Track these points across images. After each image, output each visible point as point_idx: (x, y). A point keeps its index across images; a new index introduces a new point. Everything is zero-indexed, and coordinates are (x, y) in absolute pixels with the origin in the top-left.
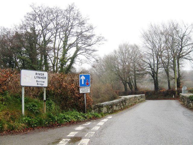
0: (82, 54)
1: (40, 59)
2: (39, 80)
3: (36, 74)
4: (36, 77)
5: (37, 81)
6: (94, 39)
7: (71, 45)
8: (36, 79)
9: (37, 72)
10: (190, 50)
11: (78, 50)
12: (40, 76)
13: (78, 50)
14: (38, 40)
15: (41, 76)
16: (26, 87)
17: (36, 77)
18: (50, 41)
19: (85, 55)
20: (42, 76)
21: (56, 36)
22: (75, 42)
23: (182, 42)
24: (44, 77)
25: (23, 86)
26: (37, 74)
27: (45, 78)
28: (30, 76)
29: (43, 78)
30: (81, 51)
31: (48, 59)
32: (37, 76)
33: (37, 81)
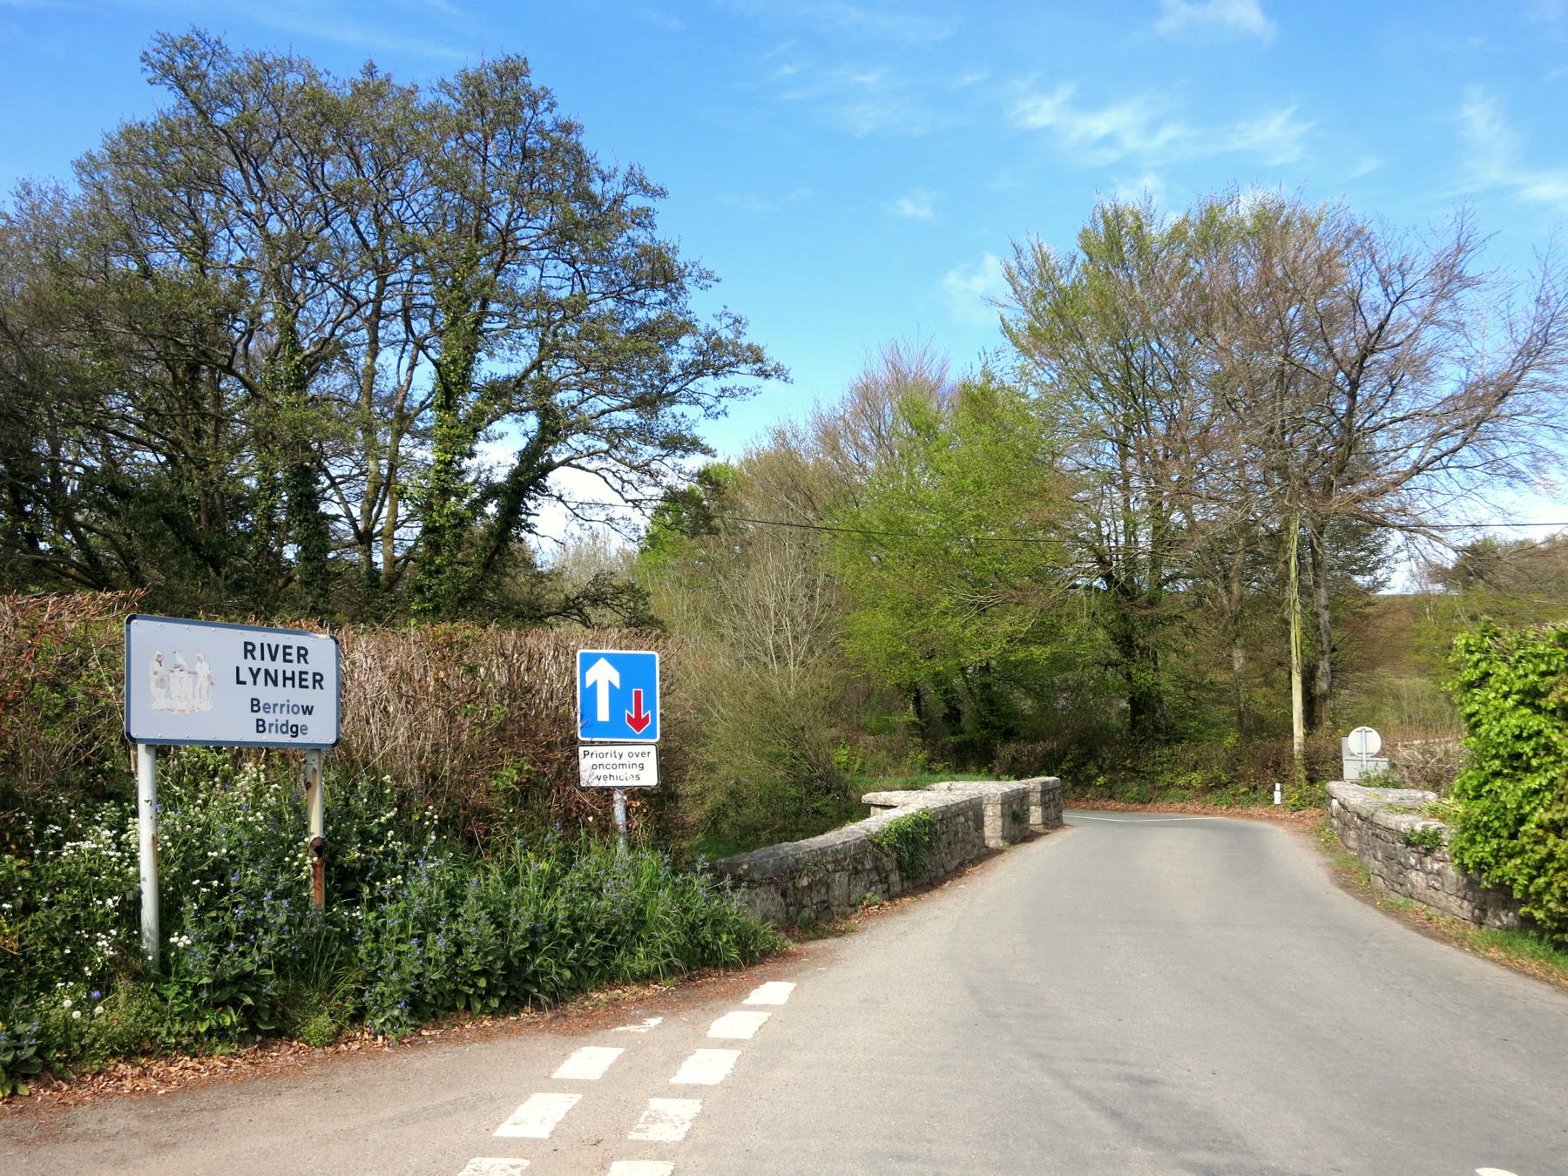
0: (583, 462)
1: (251, 482)
2: (267, 694)
3: (249, 649)
4: (246, 676)
5: (255, 704)
6: (684, 352)
7: (502, 395)
8: (250, 691)
9: (257, 637)
10: (1414, 454)
11: (552, 429)
12: (279, 665)
13: (552, 429)
14: (240, 347)
15: (289, 668)
16: (161, 750)
17: (246, 676)
18: (329, 352)
19: (609, 476)
20: (297, 667)
21: (377, 313)
22: (527, 372)
23: (1352, 396)
24: (310, 677)
25: (142, 741)
26: (257, 653)
27: (318, 680)
28: (203, 669)
29: (299, 680)
30: (577, 441)
31: (324, 490)
32: (256, 664)
33: (255, 704)
